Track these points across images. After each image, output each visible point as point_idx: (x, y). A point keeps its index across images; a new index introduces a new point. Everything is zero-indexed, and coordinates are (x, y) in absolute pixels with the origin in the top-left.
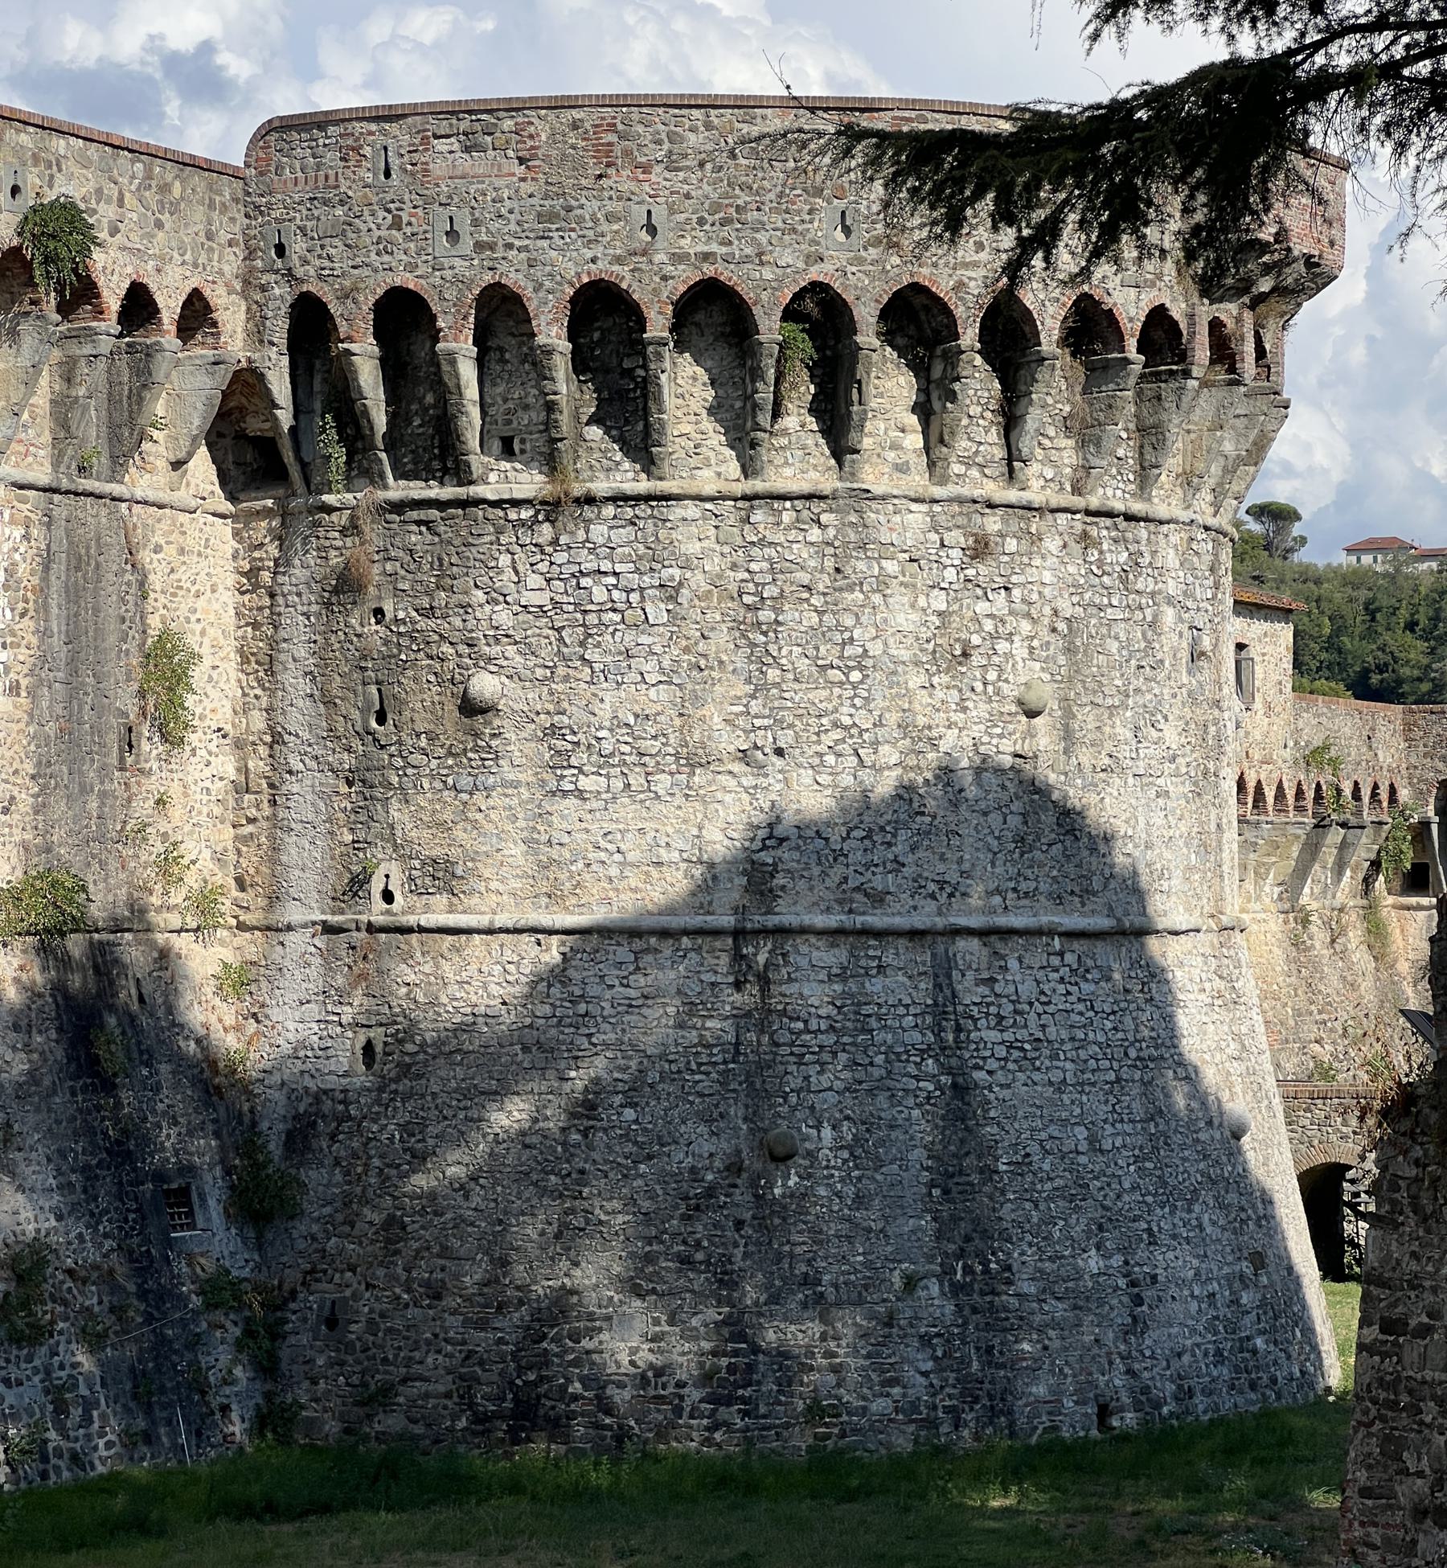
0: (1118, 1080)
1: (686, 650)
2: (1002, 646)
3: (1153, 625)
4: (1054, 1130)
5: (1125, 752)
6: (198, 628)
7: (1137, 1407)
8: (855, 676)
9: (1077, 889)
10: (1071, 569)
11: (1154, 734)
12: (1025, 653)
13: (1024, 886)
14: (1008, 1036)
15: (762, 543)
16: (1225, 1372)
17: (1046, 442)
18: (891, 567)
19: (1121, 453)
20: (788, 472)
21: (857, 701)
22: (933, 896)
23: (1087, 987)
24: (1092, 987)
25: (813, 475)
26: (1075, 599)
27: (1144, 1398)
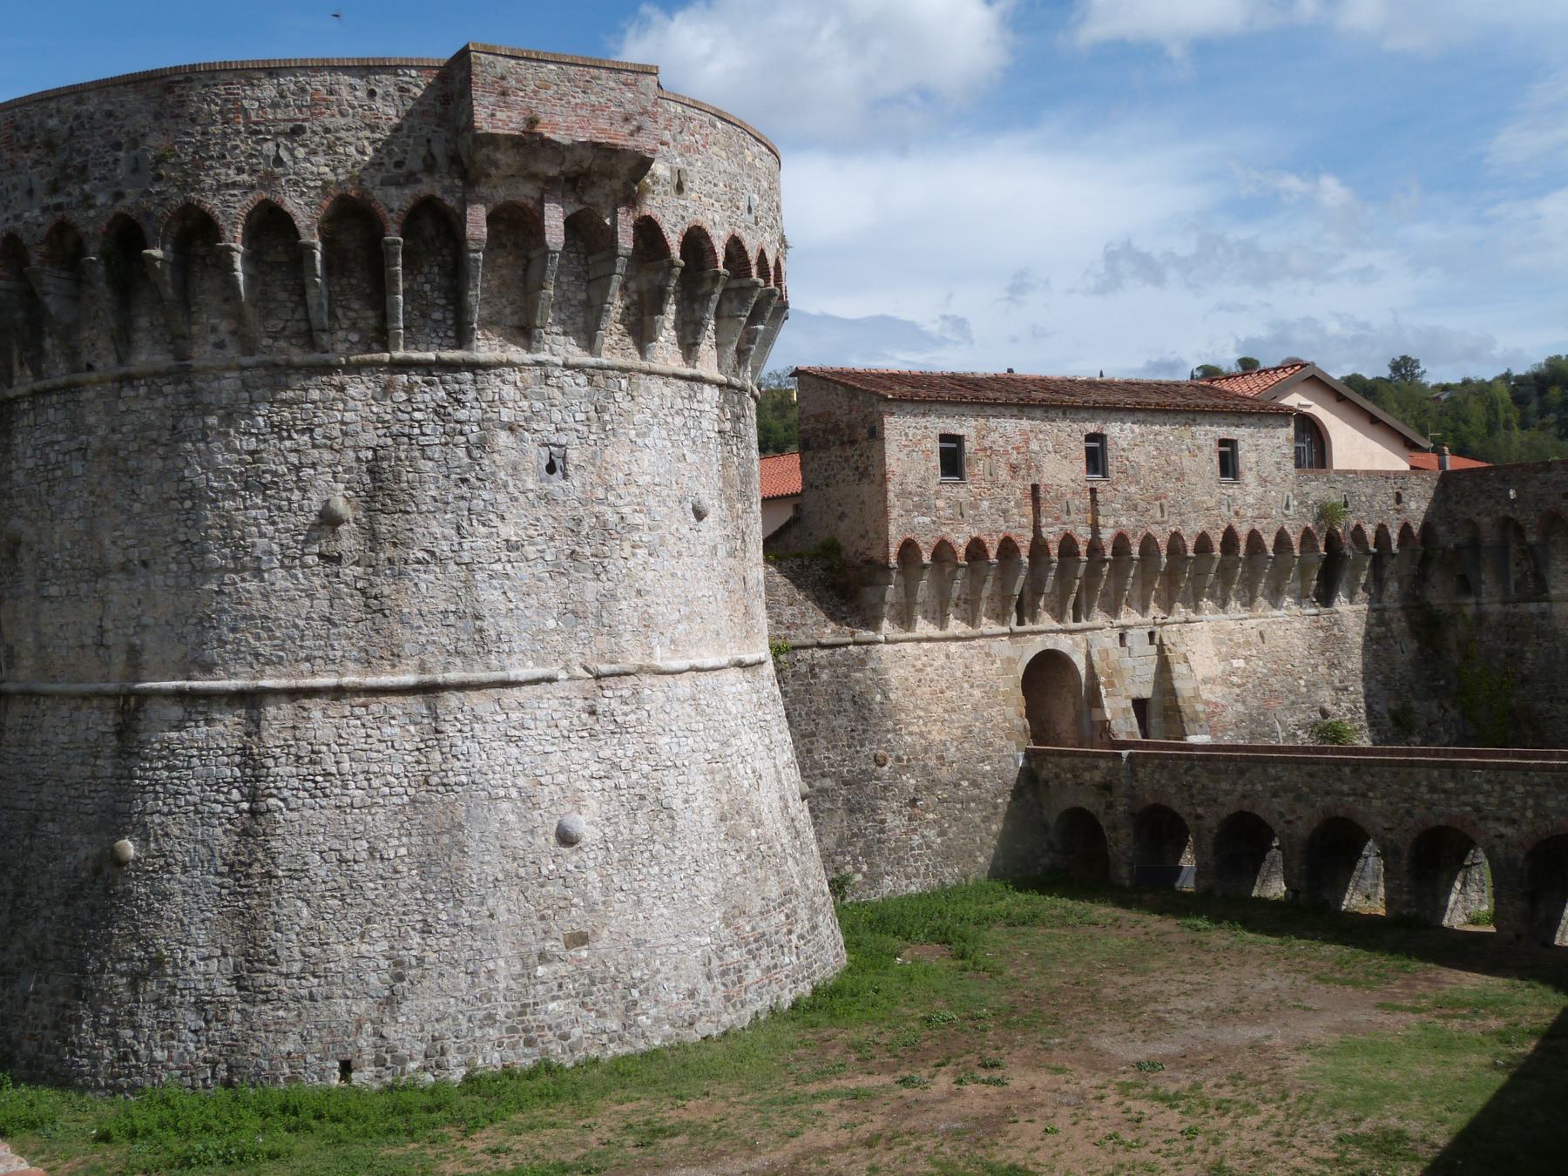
0: (413, 801)
1: (92, 493)
3: (482, 444)
4: (337, 844)
7: (379, 1062)
8: (188, 504)
9: (387, 654)
11: (483, 530)
14: (304, 771)
15: (129, 411)
16: (493, 1033)
17: (352, 314)
18: (213, 420)
19: (437, 315)
21: (189, 523)
23: (387, 730)
24: (397, 730)
25: (158, 358)
26: (381, 432)
27: (387, 1057)
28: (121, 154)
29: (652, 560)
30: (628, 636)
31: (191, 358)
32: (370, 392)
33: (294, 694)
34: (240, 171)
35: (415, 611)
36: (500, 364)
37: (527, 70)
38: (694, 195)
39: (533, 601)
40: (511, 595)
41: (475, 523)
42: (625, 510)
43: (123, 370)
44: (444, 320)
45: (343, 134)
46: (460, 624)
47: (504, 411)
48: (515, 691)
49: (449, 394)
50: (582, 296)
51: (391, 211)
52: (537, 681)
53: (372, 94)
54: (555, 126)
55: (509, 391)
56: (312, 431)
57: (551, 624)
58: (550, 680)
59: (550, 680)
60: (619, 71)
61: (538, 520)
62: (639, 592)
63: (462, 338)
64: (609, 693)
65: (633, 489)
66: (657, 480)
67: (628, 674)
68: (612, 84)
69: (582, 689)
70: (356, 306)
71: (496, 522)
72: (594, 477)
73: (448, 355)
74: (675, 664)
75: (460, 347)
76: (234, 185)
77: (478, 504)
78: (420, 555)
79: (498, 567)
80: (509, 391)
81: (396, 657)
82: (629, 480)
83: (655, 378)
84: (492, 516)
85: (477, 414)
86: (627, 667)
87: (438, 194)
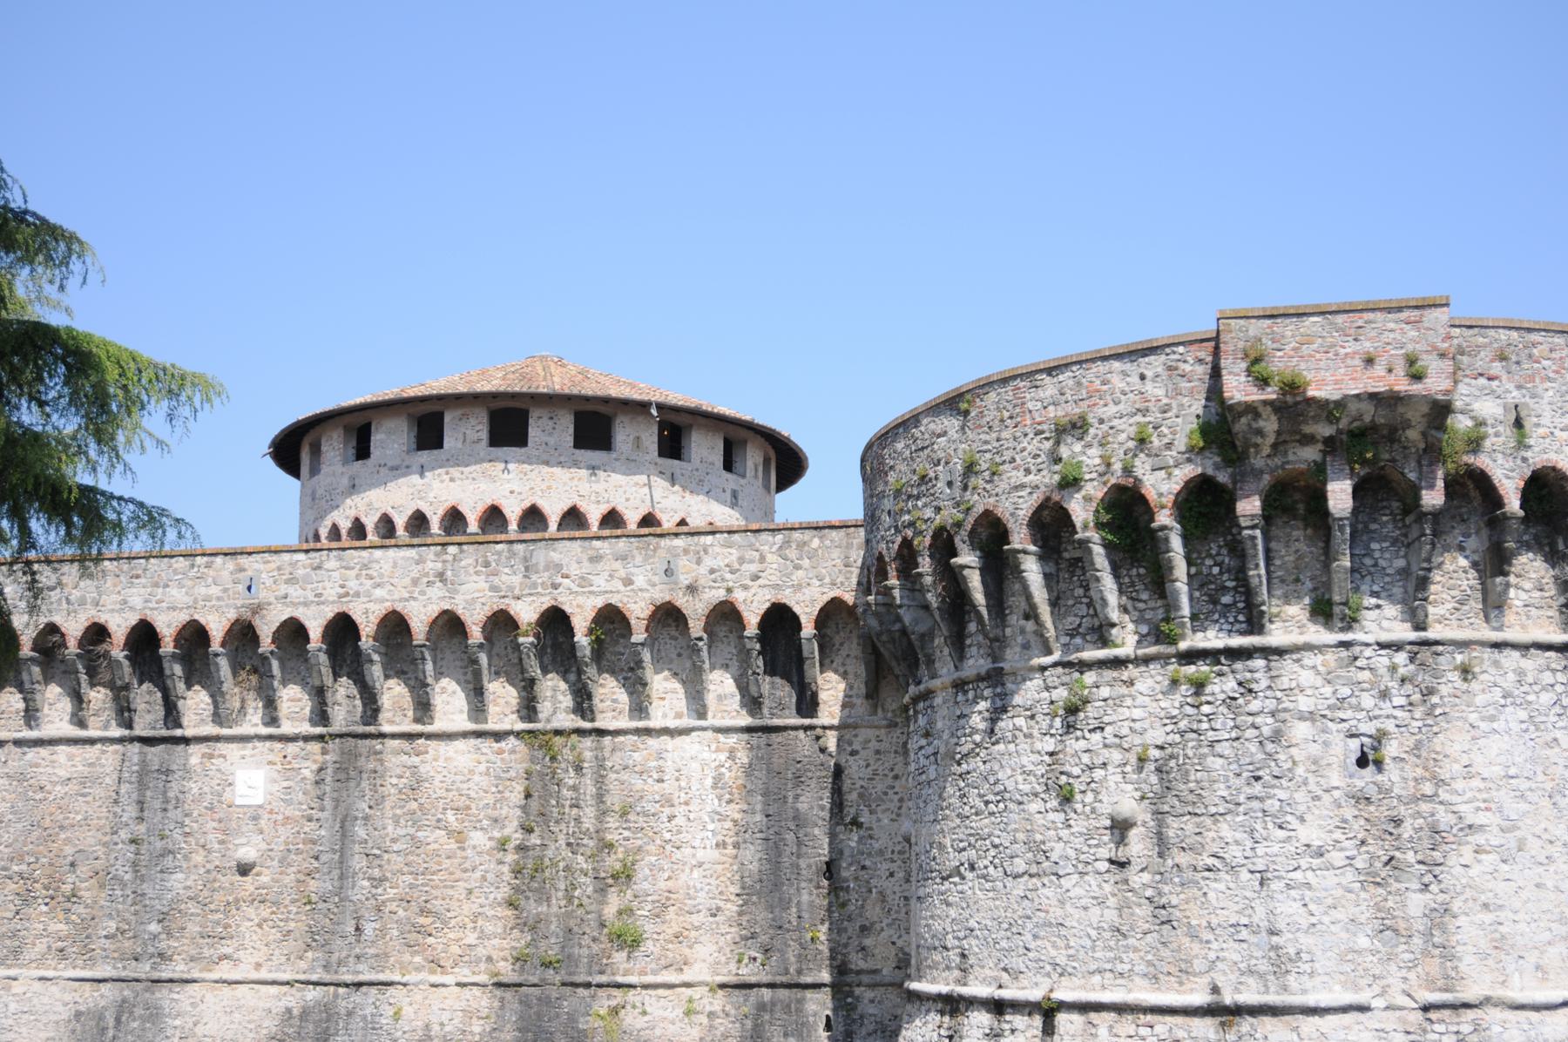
2: (1098, 774)
3: (1276, 737)
5: (1234, 854)
6: (896, 798)
10: (1163, 704)
11: (1281, 834)
12: (1119, 778)
13: (1119, 967)
17: (1141, 606)
18: (1020, 722)
19: (1226, 599)
20: (971, 662)
22: (1048, 975)
25: (982, 661)
28: (940, 468)
29: (1505, 867)
30: (1468, 959)
31: (1004, 660)
32: (1158, 687)
33: (1084, 1008)
34: (1028, 471)
35: (1205, 924)
36: (1296, 649)
37: (1288, 328)
38: (1541, 431)
39: (1339, 914)
40: (1312, 907)
41: (1270, 825)
42: (1462, 808)
43: (956, 675)
44: (1235, 603)
45: (1115, 422)
46: (1253, 939)
47: (1301, 698)
48: (1316, 1020)
49: (1240, 684)
50: (1401, 563)
51: (1160, 495)
52: (1345, 1009)
53: (1143, 377)
54: (1323, 382)
55: (1306, 677)
56: (1102, 729)
57: (1363, 942)
58: (1363, 1009)
59: (1363, 1009)
60: (1400, 309)
61: (1345, 821)
62: (1486, 906)
63: (1255, 623)
64: (1437, 1027)
65: (1476, 783)
66: (1512, 772)
67: (1467, 1006)
68: (1392, 325)
69: (1403, 1021)
70: (1144, 596)
71: (1295, 823)
72: (1419, 771)
73: (1237, 641)
74: (1541, 997)
75: (1250, 632)
76: (1022, 486)
77: (1272, 805)
78: (1210, 861)
79: (1298, 875)
80: (1306, 677)
81: (1185, 972)
82: (1469, 772)
83: (1507, 652)
84: (1289, 818)
85: (1271, 704)
86: (1469, 995)
87: (1210, 472)
